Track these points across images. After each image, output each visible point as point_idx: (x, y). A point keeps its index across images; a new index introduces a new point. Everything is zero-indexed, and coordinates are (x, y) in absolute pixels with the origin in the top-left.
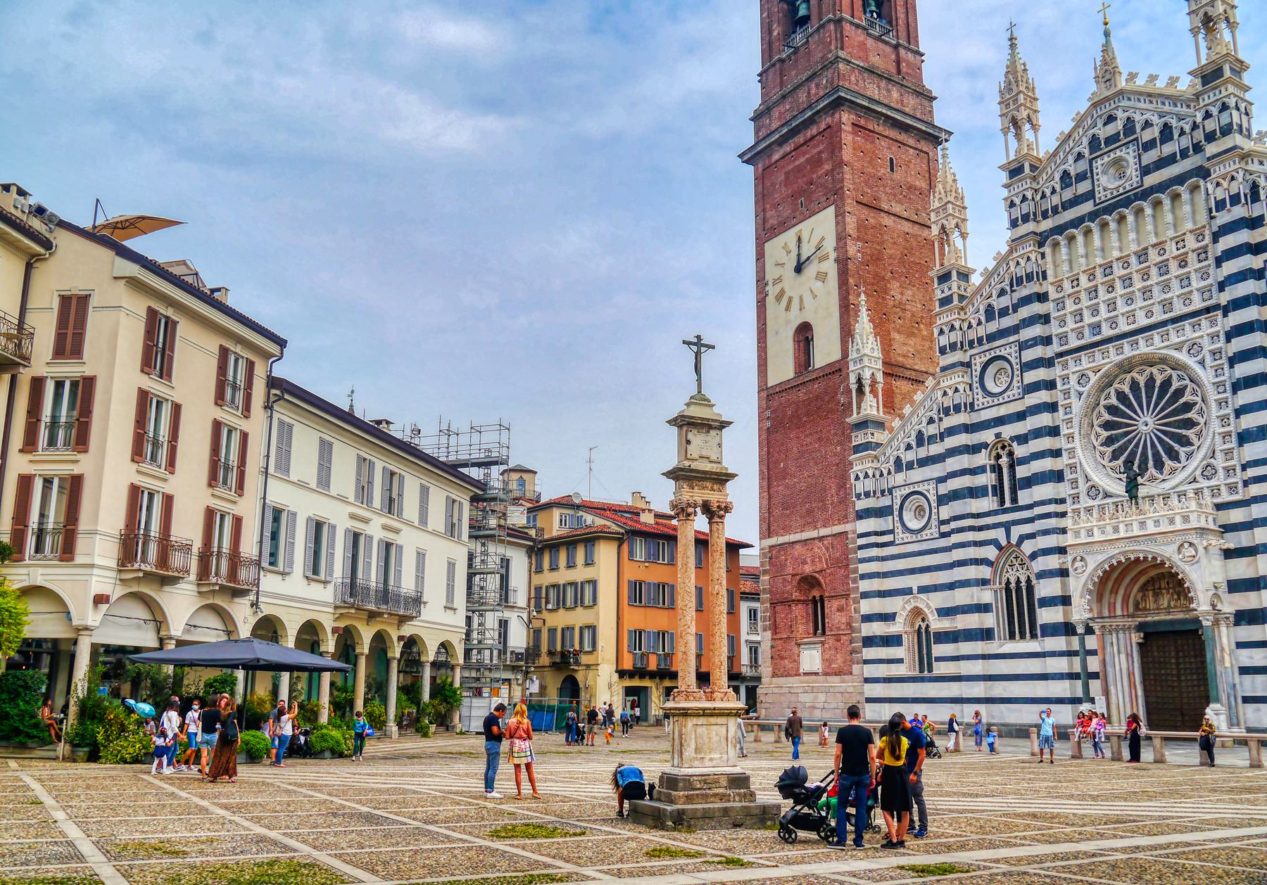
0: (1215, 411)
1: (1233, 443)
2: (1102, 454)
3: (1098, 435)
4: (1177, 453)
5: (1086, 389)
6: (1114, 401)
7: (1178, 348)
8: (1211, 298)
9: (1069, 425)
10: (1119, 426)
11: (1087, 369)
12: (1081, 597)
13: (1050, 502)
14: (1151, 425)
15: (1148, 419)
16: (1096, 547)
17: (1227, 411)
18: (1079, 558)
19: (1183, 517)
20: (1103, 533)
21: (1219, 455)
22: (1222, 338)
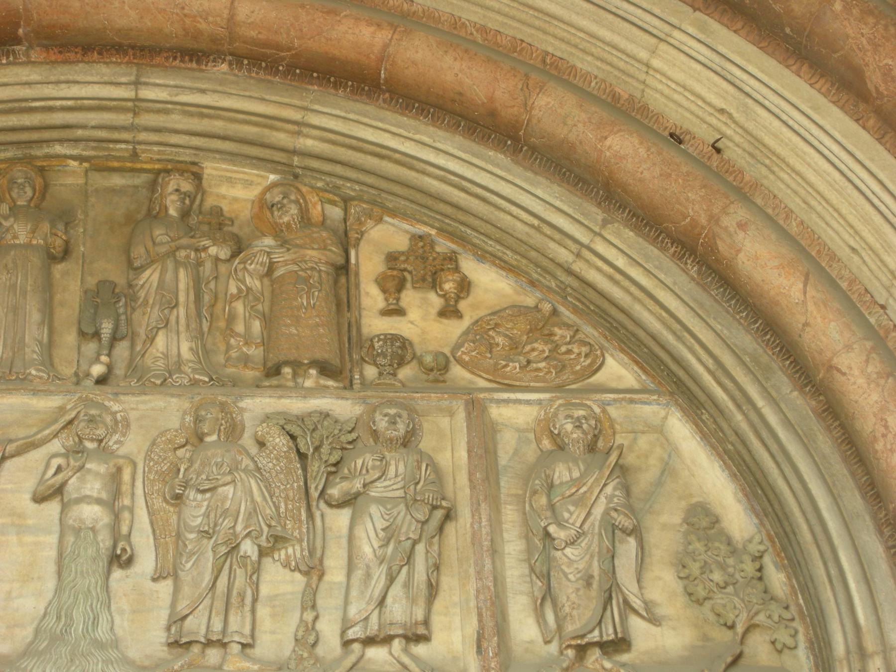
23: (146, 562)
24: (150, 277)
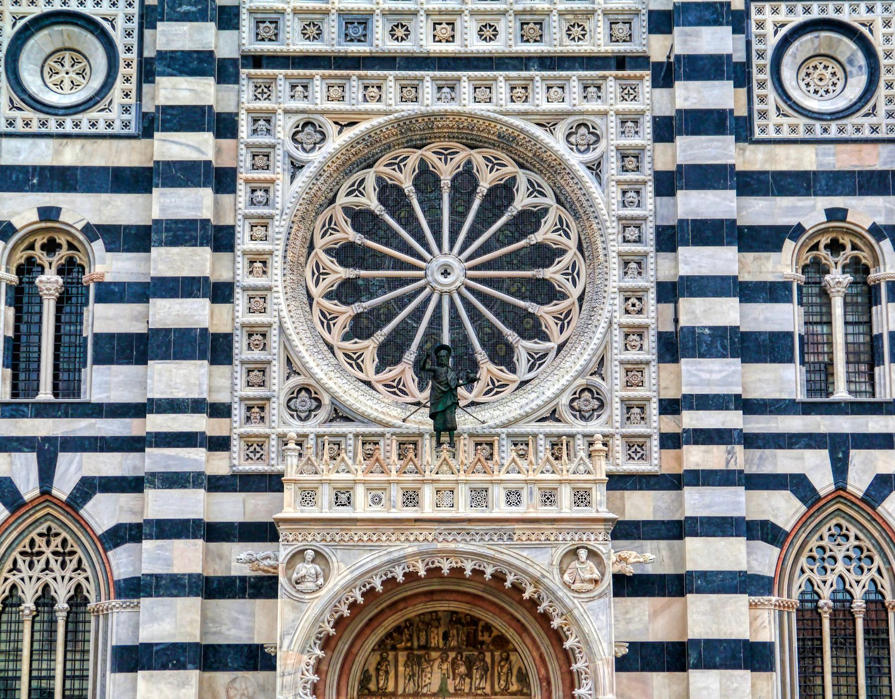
0: (615, 279)
1: (649, 349)
2: (328, 320)
3: (320, 273)
4: (510, 349)
5: (317, 157)
6: (371, 201)
7: (548, 123)
8: (629, 38)
9: (259, 232)
10: (376, 261)
11: (323, 113)
12: (302, 652)
13: (196, 406)
14: (457, 278)
15: (451, 260)
16: (359, 534)
17: (640, 283)
18: (310, 554)
19: (303, 490)
20: (376, 500)
21: (616, 374)
22: (647, 127)
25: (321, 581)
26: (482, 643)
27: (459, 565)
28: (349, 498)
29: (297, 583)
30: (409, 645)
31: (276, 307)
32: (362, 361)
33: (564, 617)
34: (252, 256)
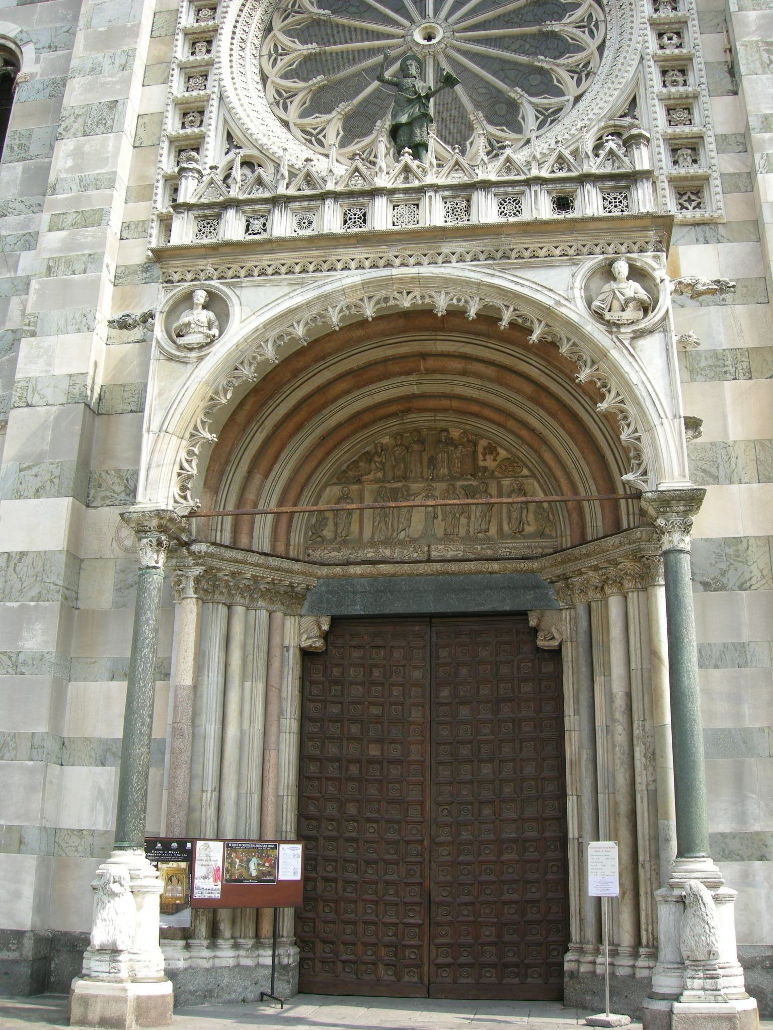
3: (277, 53)
4: (513, 106)
18: (201, 296)
23: (440, 517)
24: (440, 456)
25: (215, 331)
26: (485, 469)
27: (427, 300)
28: (264, 225)
29: (179, 336)
30: (380, 475)
31: (217, 77)
32: (324, 136)
33: (595, 367)
34: (194, 36)
